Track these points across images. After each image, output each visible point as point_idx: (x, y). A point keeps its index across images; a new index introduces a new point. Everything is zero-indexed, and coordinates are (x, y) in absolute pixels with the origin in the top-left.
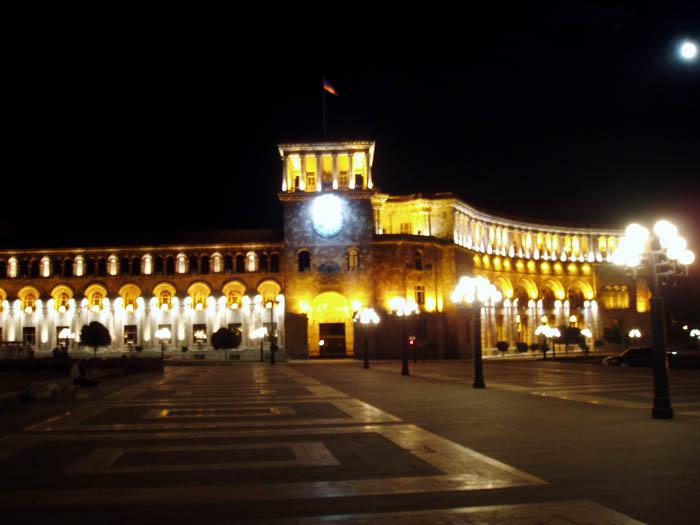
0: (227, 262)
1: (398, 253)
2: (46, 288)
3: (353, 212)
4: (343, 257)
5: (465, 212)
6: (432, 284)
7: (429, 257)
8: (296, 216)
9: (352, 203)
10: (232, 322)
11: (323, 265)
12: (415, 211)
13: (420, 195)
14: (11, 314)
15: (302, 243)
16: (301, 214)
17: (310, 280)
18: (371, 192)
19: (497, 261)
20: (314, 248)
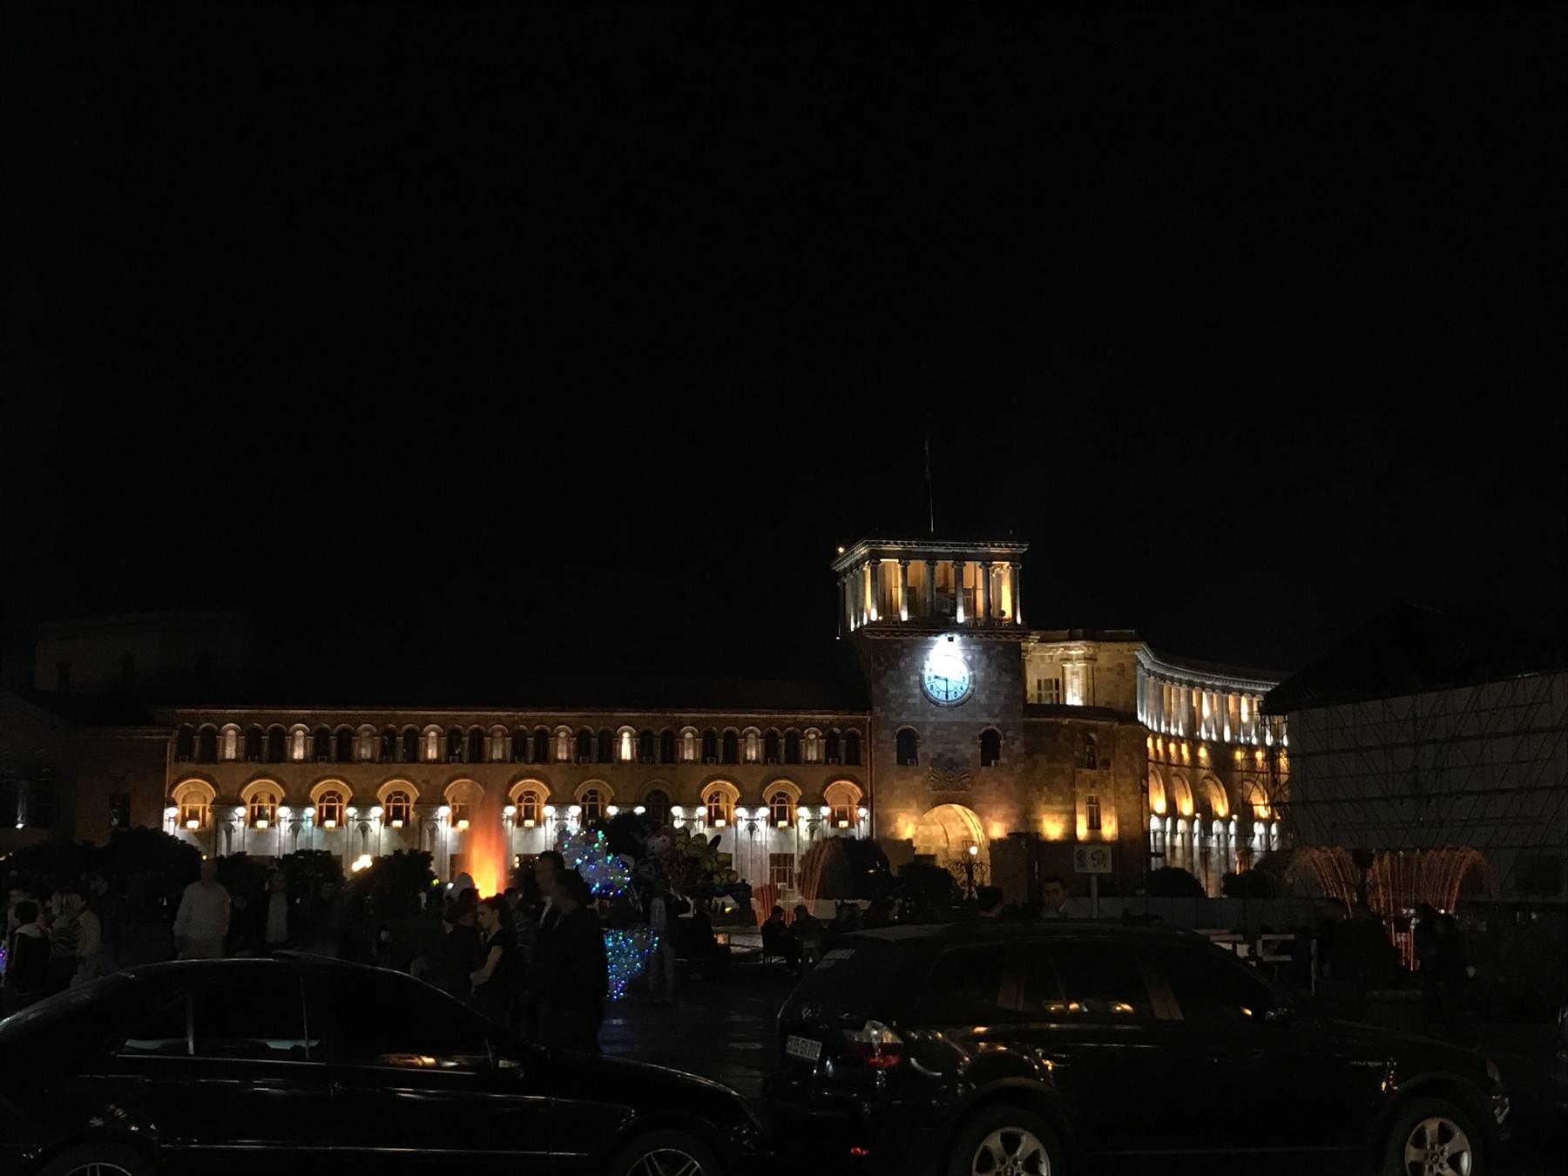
0: (770, 752)
1: (1061, 740)
2: (433, 782)
3: (988, 665)
4: (973, 742)
5: (1145, 658)
6: (1110, 794)
7: (1097, 744)
8: (893, 666)
9: (987, 650)
10: (776, 851)
11: (940, 755)
12: (1068, 659)
13: (1080, 631)
14: (364, 829)
15: (904, 717)
16: (902, 664)
17: (917, 780)
18: (1023, 632)
19: (1172, 747)
20: (922, 725)
